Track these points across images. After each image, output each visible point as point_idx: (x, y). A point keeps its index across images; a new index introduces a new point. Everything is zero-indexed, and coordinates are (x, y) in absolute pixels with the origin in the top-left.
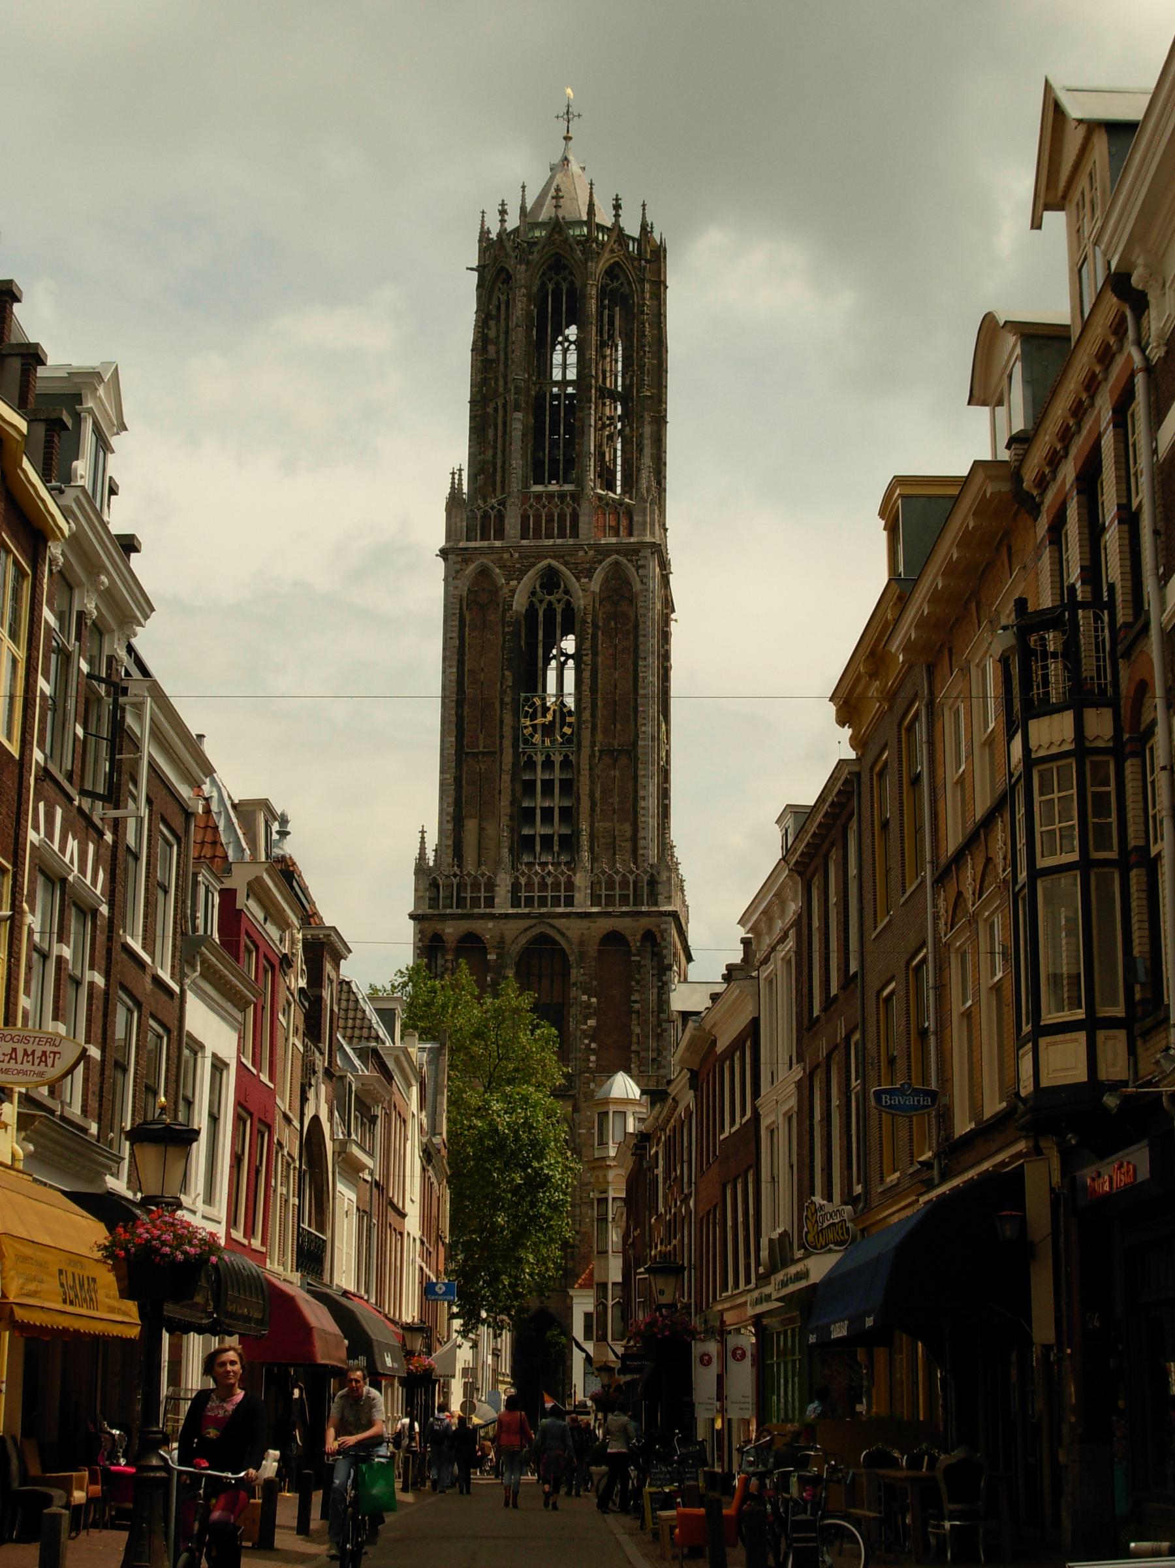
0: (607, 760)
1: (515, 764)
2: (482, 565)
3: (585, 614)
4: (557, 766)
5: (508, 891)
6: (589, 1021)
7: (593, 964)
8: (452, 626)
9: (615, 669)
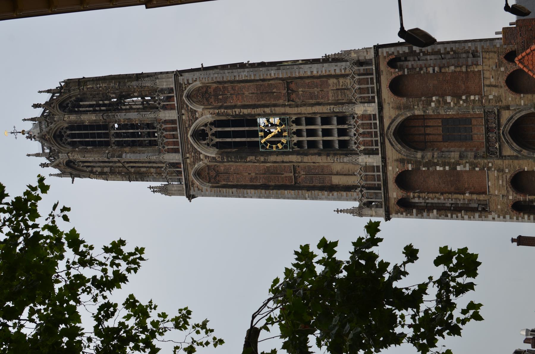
0: (294, 96)
1: (298, 153)
2: (195, 175)
3: (214, 114)
4: (299, 127)
5: (369, 157)
6: (448, 101)
7: (411, 99)
8: (226, 193)
9: (244, 94)
